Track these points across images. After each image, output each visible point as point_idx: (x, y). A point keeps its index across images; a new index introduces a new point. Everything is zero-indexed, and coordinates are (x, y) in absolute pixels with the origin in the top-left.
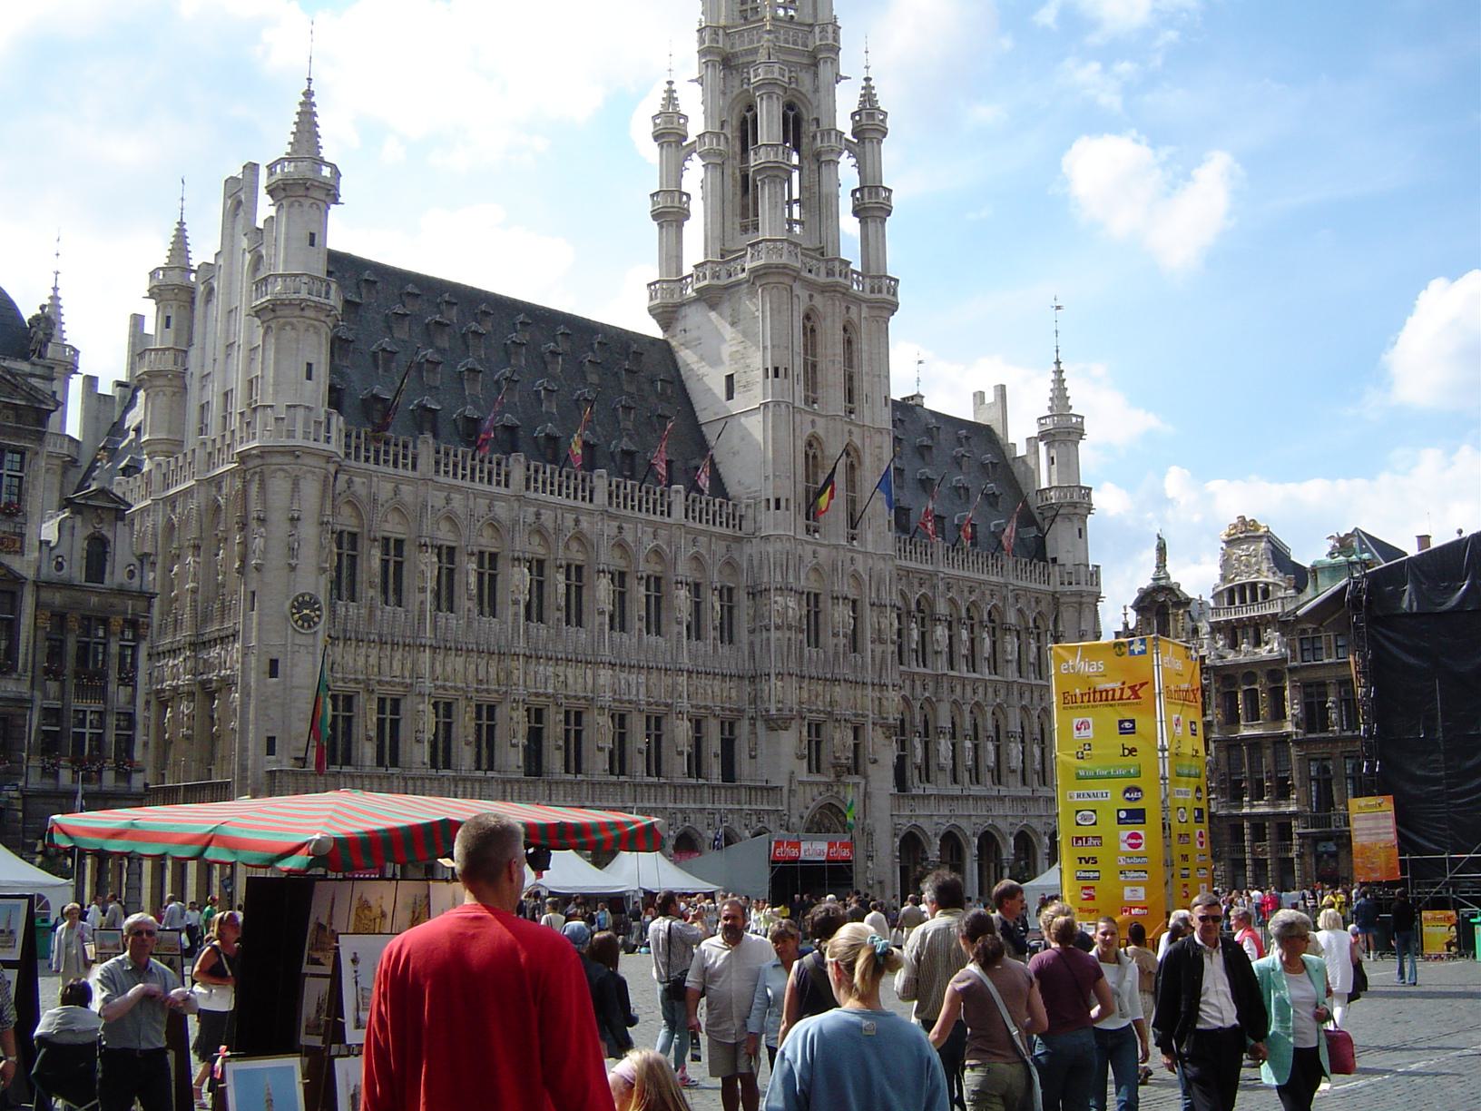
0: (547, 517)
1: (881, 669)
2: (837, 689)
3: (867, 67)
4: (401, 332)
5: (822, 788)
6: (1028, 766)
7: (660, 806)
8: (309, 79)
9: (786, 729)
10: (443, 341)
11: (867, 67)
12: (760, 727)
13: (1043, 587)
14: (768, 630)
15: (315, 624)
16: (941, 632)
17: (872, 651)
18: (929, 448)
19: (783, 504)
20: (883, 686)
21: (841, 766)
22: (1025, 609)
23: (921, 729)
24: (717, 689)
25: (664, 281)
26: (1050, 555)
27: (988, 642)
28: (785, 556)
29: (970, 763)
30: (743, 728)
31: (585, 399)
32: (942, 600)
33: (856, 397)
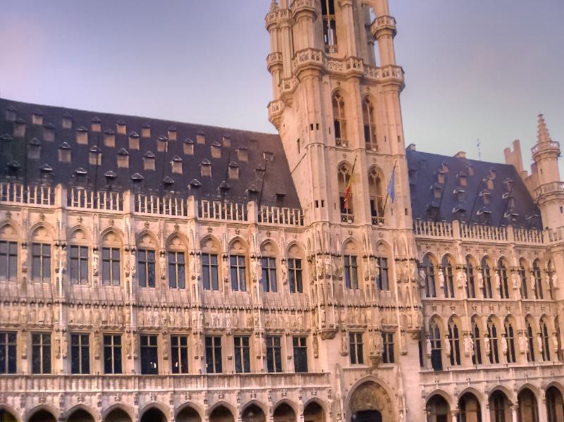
0: (155, 227)
5: (364, 372)
9: (331, 338)
12: (319, 338)
13: (538, 244)
14: (316, 280)
16: (461, 277)
17: (399, 288)
19: (320, 203)
21: (376, 358)
22: (526, 257)
23: (448, 334)
24: (286, 319)
25: (274, 102)
26: (544, 227)
27: (498, 278)
28: (321, 235)
29: (489, 351)
30: (310, 339)
32: (460, 256)
33: (378, 139)
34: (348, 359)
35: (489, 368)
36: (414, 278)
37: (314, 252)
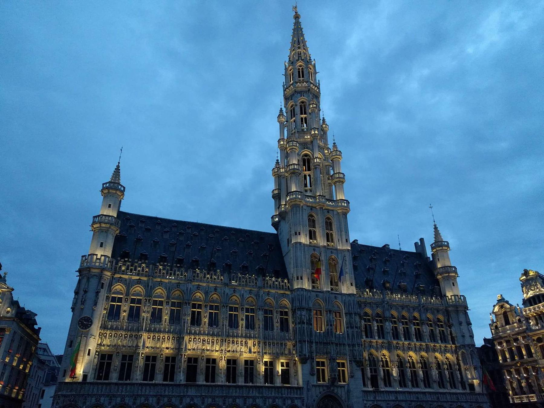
1: (352, 339)
2: (329, 347)
3: (334, 140)
4: (166, 236)
5: (325, 388)
6: (444, 380)
7: (241, 395)
8: (119, 163)
10: (181, 238)
11: (334, 140)
15: (89, 327)
17: (347, 331)
18: (388, 261)
20: (353, 345)
28: (300, 297)
31: (233, 251)
34: (315, 377)
35: (411, 390)
36: (357, 325)
37: (296, 307)
